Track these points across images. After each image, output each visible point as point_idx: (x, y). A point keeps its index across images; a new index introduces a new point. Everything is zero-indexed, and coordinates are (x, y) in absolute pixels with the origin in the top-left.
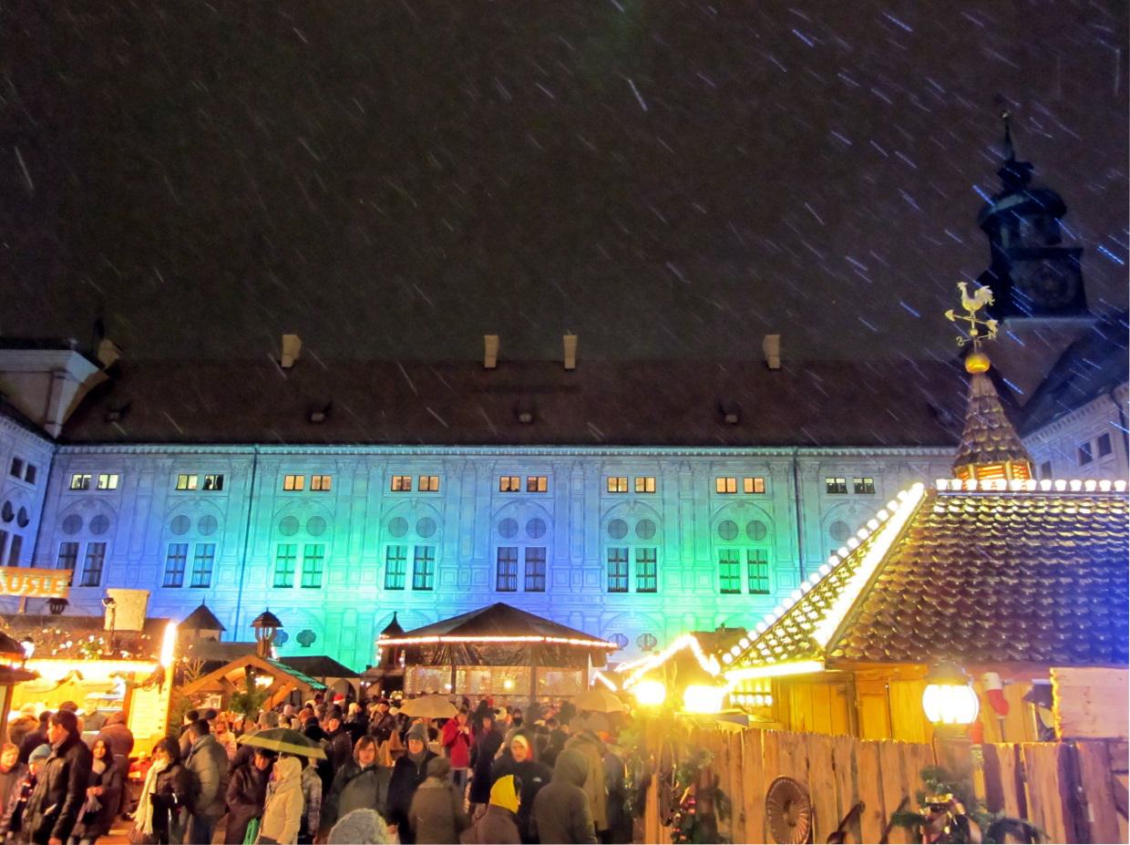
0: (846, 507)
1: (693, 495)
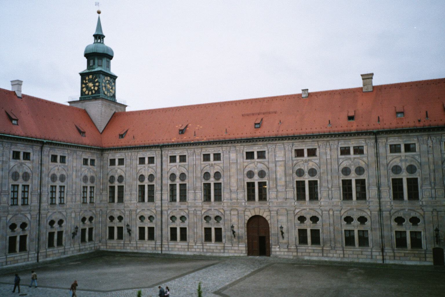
0: (57, 168)
1: (3, 158)
